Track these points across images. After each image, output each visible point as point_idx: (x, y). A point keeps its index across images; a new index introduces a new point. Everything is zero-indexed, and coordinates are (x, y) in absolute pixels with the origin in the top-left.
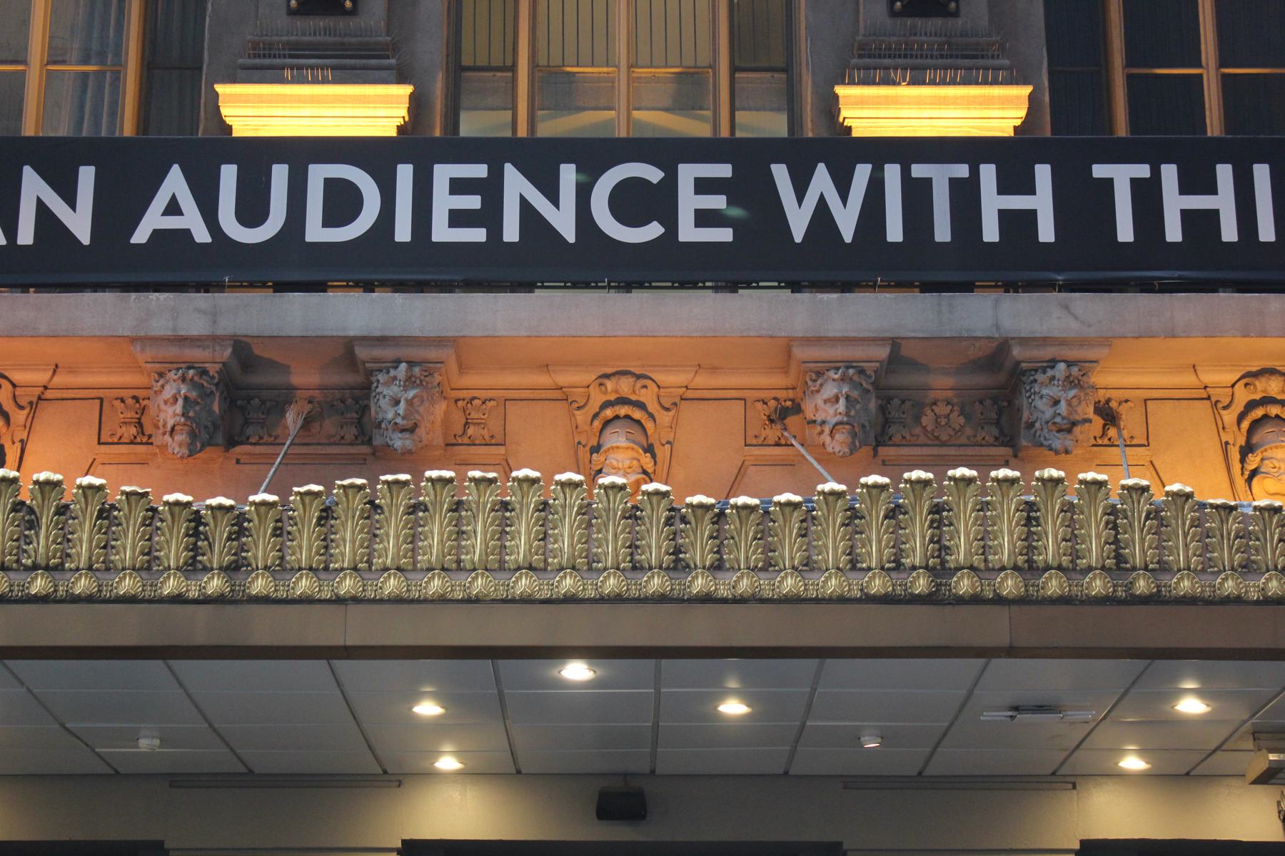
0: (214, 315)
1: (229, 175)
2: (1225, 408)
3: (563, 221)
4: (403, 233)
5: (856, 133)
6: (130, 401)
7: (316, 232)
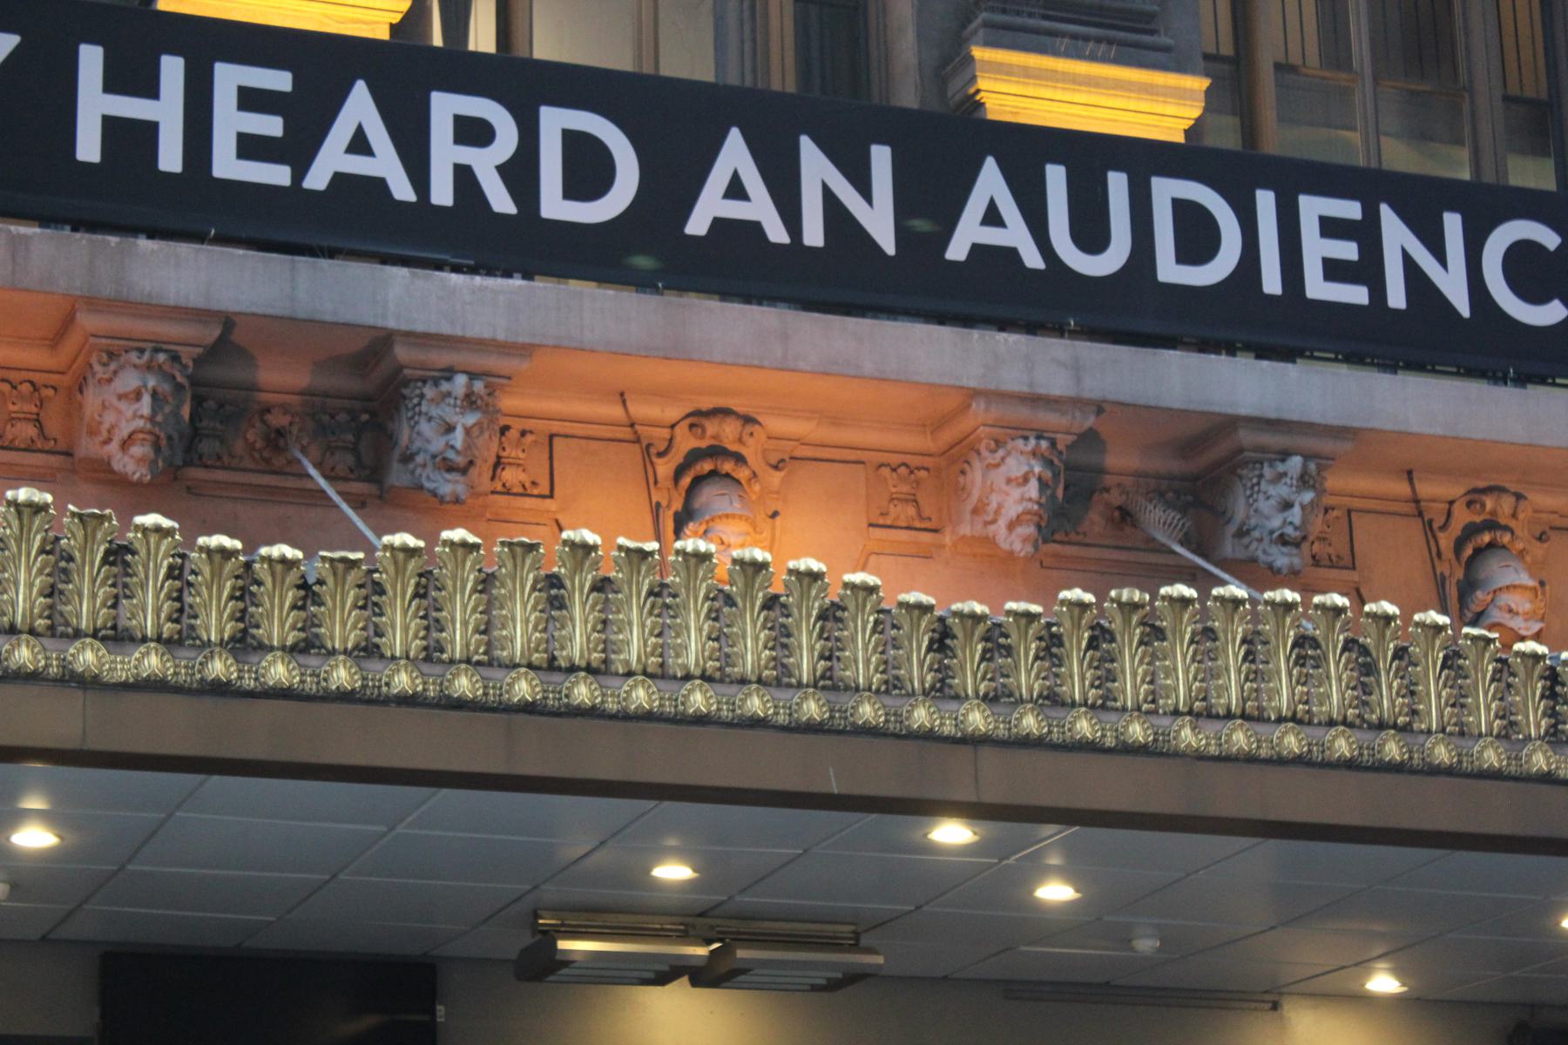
0: (1077, 369)
1: (1056, 178)
2: (660, 455)
3: (1453, 286)
4: (1272, 283)
5: (991, 116)
6: (26, 388)
7: (1169, 270)
